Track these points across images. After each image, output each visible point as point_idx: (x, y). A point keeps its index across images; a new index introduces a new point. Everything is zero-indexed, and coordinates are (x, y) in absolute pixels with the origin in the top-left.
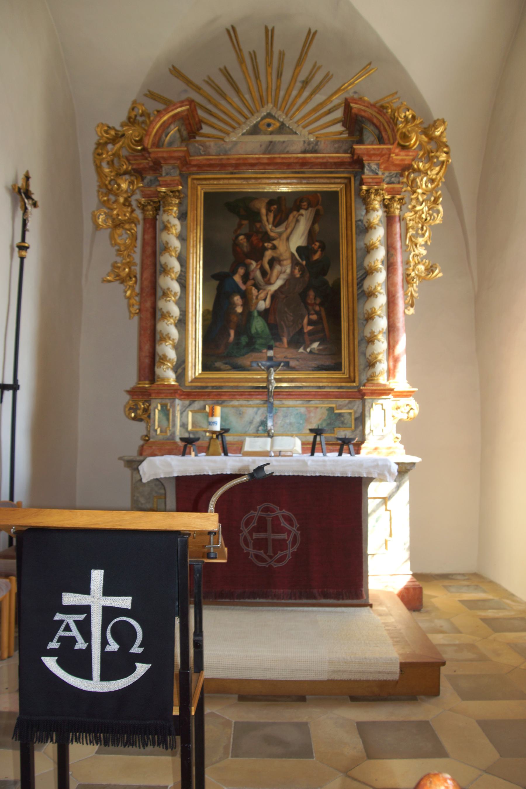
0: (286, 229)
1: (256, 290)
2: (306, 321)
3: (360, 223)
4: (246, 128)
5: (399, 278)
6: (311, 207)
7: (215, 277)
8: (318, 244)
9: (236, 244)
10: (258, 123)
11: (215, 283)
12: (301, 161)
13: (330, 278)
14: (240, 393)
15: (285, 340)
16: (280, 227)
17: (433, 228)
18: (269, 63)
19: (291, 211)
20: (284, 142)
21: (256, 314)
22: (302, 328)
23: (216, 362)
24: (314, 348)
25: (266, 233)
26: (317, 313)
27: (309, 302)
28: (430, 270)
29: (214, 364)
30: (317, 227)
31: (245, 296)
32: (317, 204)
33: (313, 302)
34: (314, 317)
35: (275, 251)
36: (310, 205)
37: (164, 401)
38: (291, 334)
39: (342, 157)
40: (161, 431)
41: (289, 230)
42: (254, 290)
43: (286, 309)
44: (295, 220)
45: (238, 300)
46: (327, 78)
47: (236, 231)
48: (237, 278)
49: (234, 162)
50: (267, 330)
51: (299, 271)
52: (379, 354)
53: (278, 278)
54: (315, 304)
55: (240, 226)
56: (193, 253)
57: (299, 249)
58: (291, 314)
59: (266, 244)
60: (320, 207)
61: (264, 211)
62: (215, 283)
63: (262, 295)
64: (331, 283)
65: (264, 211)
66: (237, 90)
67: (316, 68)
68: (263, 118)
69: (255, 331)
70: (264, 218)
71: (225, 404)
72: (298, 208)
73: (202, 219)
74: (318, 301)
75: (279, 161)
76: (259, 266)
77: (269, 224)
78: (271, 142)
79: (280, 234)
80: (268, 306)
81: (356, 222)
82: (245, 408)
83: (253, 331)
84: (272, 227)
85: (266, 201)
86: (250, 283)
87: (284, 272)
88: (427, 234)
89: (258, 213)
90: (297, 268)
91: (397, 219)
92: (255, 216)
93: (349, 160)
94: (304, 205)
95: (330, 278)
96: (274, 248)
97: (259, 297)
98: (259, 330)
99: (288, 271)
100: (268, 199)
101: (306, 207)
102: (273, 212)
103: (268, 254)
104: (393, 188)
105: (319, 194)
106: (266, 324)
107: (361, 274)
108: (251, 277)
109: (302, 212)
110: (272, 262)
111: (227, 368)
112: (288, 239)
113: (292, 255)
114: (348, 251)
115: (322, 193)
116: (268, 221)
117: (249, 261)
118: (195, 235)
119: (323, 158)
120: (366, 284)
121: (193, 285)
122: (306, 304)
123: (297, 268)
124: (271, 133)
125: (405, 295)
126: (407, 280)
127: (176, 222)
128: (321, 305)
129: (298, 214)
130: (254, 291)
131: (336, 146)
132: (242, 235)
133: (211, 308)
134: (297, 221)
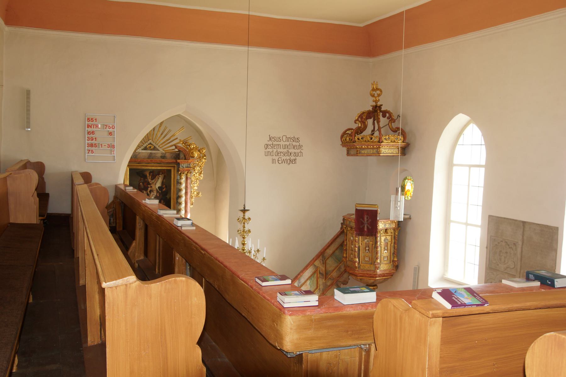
0: (155, 181)
5: (189, 196)
8: (165, 186)
10: (146, 147)
13: (168, 197)
17: (200, 181)
19: (157, 175)
20: (155, 153)
25: (149, 182)
28: (198, 194)
30: (164, 180)
32: (164, 173)
41: (156, 181)
46: (170, 131)
49: (139, 161)
53: (152, 196)
55: (141, 180)
57: (159, 187)
60: (165, 174)
61: (148, 175)
65: (148, 175)
70: (148, 177)
78: (151, 153)
79: (153, 182)
81: (177, 180)
87: (154, 195)
88: (197, 183)
91: (189, 178)
92: (145, 177)
95: (168, 197)
96: (151, 187)
99: (155, 194)
103: (149, 189)
104: (188, 169)
109: (160, 175)
110: (150, 191)
112: (155, 184)
113: (157, 189)
116: (149, 178)
120: (179, 201)
124: (151, 150)
125: (190, 201)
126: (191, 197)
131: (171, 155)
132: (141, 182)
134: (158, 178)
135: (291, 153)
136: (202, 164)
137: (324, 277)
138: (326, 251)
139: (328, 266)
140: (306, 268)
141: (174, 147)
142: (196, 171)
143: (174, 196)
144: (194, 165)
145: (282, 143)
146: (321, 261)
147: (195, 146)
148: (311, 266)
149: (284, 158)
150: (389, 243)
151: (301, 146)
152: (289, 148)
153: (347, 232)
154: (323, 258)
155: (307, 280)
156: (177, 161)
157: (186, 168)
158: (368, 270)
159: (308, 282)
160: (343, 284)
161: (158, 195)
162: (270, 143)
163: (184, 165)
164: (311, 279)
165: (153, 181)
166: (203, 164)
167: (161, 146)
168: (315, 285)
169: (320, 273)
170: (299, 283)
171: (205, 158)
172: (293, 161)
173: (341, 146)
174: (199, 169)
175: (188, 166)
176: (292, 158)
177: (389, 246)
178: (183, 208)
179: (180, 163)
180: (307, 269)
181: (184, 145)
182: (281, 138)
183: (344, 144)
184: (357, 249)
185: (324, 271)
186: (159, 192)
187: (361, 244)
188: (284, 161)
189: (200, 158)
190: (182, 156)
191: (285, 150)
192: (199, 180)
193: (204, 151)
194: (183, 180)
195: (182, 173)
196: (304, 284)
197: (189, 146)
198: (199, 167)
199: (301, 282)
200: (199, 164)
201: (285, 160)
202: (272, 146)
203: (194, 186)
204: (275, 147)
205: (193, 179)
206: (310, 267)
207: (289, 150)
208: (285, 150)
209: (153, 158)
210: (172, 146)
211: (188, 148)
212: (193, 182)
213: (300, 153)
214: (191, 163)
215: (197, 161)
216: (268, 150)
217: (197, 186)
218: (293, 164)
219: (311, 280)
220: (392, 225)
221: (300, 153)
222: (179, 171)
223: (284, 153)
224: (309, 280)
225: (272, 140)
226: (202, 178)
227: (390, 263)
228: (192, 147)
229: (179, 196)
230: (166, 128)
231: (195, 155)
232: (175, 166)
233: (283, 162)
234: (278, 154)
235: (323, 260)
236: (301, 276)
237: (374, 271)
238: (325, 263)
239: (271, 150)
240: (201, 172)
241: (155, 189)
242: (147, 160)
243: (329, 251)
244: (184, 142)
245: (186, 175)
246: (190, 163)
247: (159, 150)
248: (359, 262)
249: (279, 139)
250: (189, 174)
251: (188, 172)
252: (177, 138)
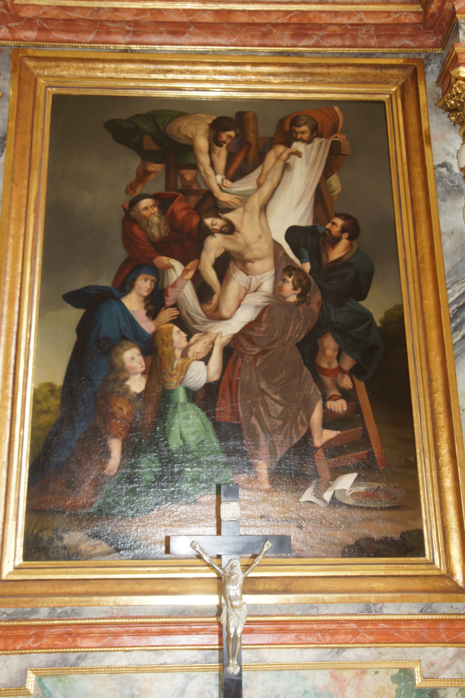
0: (259, 185)
1: (183, 335)
3: (444, 170)
6: (320, 136)
8: (339, 222)
12: (295, 20)
14: (133, 629)
16: (244, 180)
21: (181, 396)
23: (64, 531)
24: (343, 491)
25: (209, 193)
27: (324, 365)
29: (61, 539)
32: (334, 130)
33: (335, 365)
35: (230, 236)
38: (280, 453)
39: (396, 13)
41: (266, 189)
42: (178, 332)
43: (263, 385)
44: (280, 164)
45: (133, 359)
47: (131, 188)
49: (129, 18)
51: (295, 288)
54: (340, 370)
56: (16, 237)
58: (278, 398)
59: (208, 221)
60: (341, 137)
69: (181, 443)
70: (204, 159)
71: (86, 664)
73: (46, 155)
75: (242, 19)
76: (191, 274)
77: (216, 174)
80: (215, 377)
82: (147, 675)
84: (223, 180)
85: (210, 122)
90: (290, 280)
93: (413, 19)
94: (302, 133)
97: (190, 354)
98: (192, 440)
100: (215, 118)
101: (306, 136)
102: (225, 145)
105: (336, 109)
106: (209, 425)
107: (457, 295)
108: (169, 301)
109: (298, 146)
111: (98, 550)
112: (264, 209)
113: (276, 245)
114: (419, 238)
116: (212, 165)
117: (164, 260)
118: (25, 191)
119: (350, 14)
121: (10, 317)
123: (290, 280)
129: (289, 150)
133: (59, 381)
134: (287, 167)
186: (300, 271)
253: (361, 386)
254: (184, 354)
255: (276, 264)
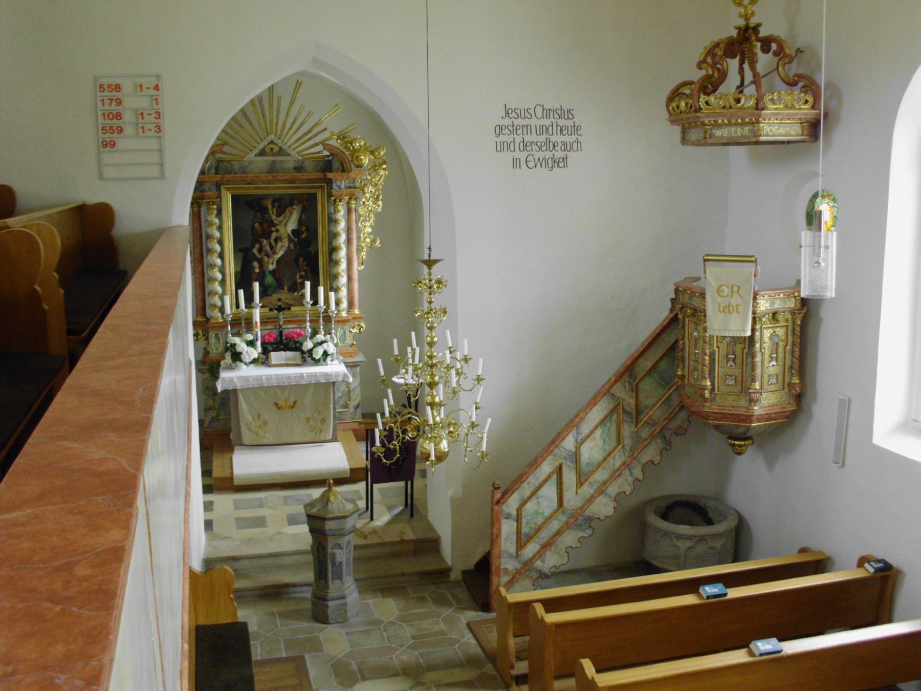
0: (285, 218)
2: (298, 276)
4: (256, 151)
7: (241, 250)
8: (304, 228)
9: (253, 228)
10: (264, 148)
11: (241, 254)
15: (286, 288)
18: (271, 105)
19: (287, 207)
20: (282, 161)
21: (267, 273)
22: (296, 281)
25: (272, 221)
26: (305, 271)
28: (373, 241)
30: (304, 216)
31: (260, 262)
34: (303, 273)
36: (299, 202)
37: (217, 332)
40: (216, 350)
41: (287, 219)
46: (310, 114)
48: (255, 251)
49: (251, 179)
50: (275, 282)
52: (342, 298)
53: (280, 250)
55: (255, 217)
57: (293, 231)
59: (272, 229)
60: (305, 204)
61: (270, 207)
62: (241, 254)
63: (271, 261)
64: (313, 252)
65: (270, 207)
66: (251, 124)
67: (302, 108)
68: (269, 143)
70: (271, 212)
72: (292, 205)
74: (305, 263)
78: (274, 161)
81: (328, 214)
83: (266, 283)
86: (263, 253)
87: (284, 246)
88: (372, 220)
89: (267, 208)
91: (353, 210)
92: (264, 210)
95: (312, 249)
96: (277, 231)
98: (270, 283)
99: (287, 245)
103: (274, 235)
108: (264, 249)
109: (295, 207)
110: (277, 240)
112: (286, 225)
113: (289, 235)
115: (307, 194)
116: (273, 213)
120: (334, 257)
122: (298, 266)
124: (274, 155)
125: (358, 258)
126: (359, 250)
127: (217, 221)
128: (307, 266)
130: (266, 259)
133: (239, 270)
134: (291, 213)
135: (556, 144)
136: (379, 181)
137: (634, 420)
138: (637, 363)
139: (641, 396)
140: (593, 402)
141: (320, 148)
142: (368, 195)
143: (324, 247)
144: (363, 183)
145: (533, 122)
146: (627, 384)
147: (363, 144)
148: (605, 397)
149: (541, 155)
150: (781, 344)
151: (576, 129)
152: (551, 133)
153: (684, 319)
154: (631, 378)
155: (596, 427)
156: (325, 175)
157: (346, 190)
158: (733, 407)
159: (598, 432)
160: (676, 434)
161: (292, 246)
162: (507, 122)
163: (341, 182)
164: (605, 425)
165: (281, 218)
166: (381, 180)
167: (293, 147)
168: (614, 437)
169: (625, 412)
170: (578, 434)
171: (384, 167)
172: (562, 162)
173: (669, 123)
174: (373, 190)
175: (352, 185)
176: (559, 154)
177: (781, 350)
178: (343, 271)
179: (333, 179)
180: (595, 404)
181: (342, 143)
182: (532, 112)
183: (675, 117)
184: (707, 358)
185: (633, 406)
187: (718, 347)
188: (540, 162)
189: (375, 168)
190: (336, 165)
191: (542, 138)
192: (374, 214)
193: (382, 153)
194: (341, 214)
195: (338, 200)
196: (588, 437)
197: (351, 143)
198: (373, 187)
199: (581, 434)
200: (374, 180)
201: (541, 160)
202: (511, 128)
203: (365, 226)
204: (519, 132)
205: (362, 210)
206: (603, 399)
207: (551, 137)
208: (542, 138)
209: (278, 172)
210: (316, 145)
211: (349, 148)
212: (362, 218)
213: (575, 144)
214: (357, 179)
215: (369, 174)
216: (502, 138)
217: (371, 226)
218: (560, 169)
219: (604, 427)
220: (788, 303)
221: (575, 144)
222: (332, 197)
223: (539, 145)
224: (599, 428)
225: (510, 116)
226: (380, 210)
227: (784, 389)
228: (358, 145)
229: (333, 247)
230: (302, 108)
231: (364, 162)
232: (324, 186)
233: (538, 165)
234: (525, 146)
235: (630, 383)
236: (582, 419)
237: (747, 408)
238: (637, 389)
239: (509, 139)
240: (378, 196)
241: (285, 235)
242: (266, 176)
243: (646, 364)
244: (341, 137)
245: (348, 203)
246: (355, 178)
247: (289, 155)
248: (713, 389)
249: (527, 113)
250: (353, 202)
251: (350, 198)
252: (325, 129)
253: (308, 269)
254: (268, 263)
255: (289, 240)
